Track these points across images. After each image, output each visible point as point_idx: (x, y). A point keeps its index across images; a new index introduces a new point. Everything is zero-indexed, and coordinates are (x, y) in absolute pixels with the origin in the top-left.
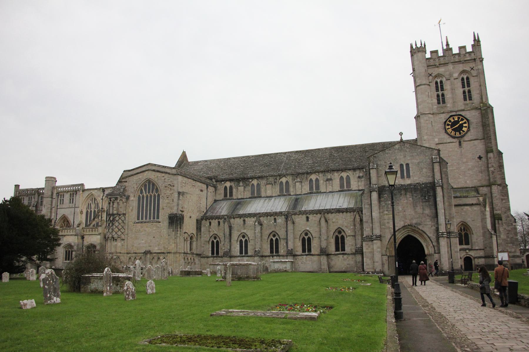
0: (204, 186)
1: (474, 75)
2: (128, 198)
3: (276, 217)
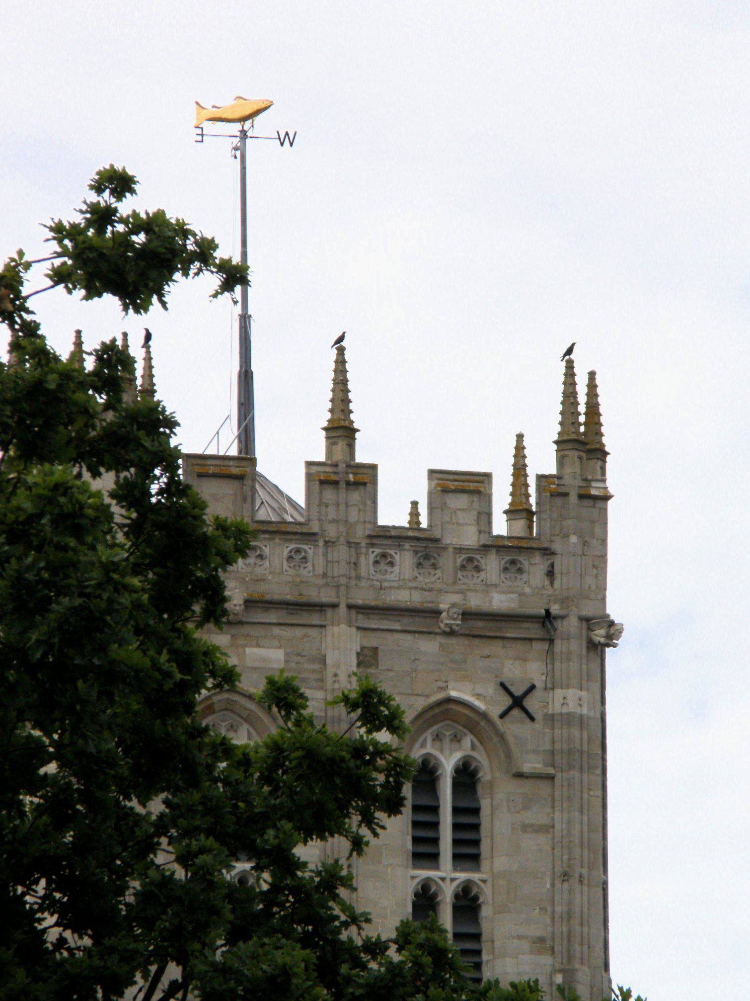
1: (527, 768)
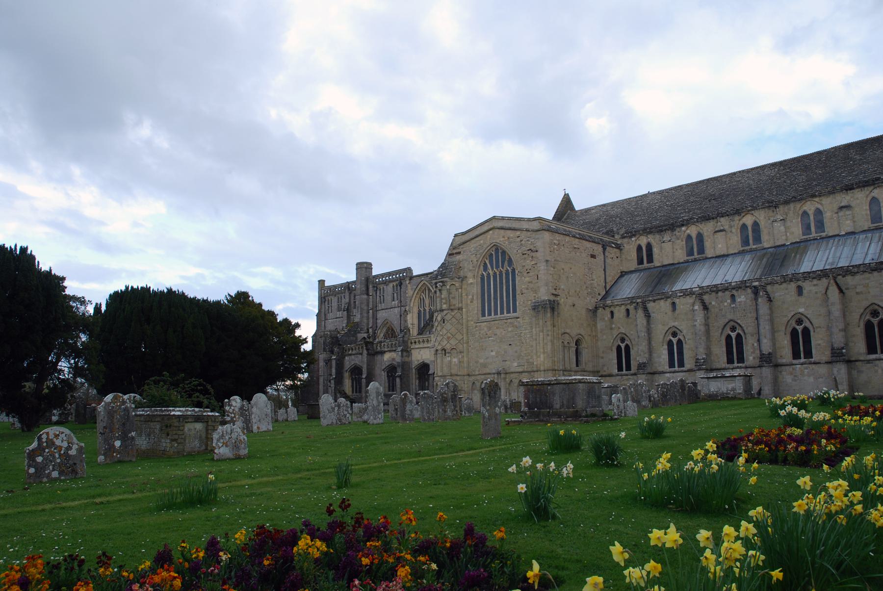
0: (598, 249)
2: (463, 279)
3: (734, 292)
